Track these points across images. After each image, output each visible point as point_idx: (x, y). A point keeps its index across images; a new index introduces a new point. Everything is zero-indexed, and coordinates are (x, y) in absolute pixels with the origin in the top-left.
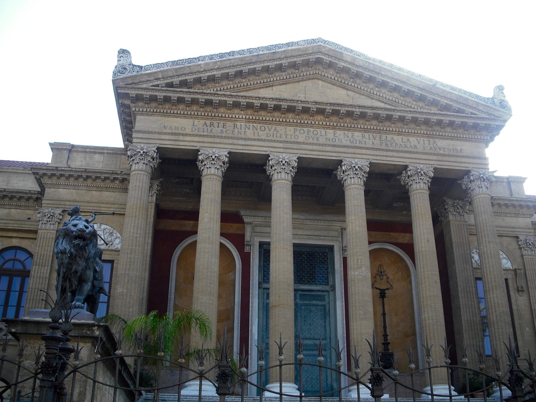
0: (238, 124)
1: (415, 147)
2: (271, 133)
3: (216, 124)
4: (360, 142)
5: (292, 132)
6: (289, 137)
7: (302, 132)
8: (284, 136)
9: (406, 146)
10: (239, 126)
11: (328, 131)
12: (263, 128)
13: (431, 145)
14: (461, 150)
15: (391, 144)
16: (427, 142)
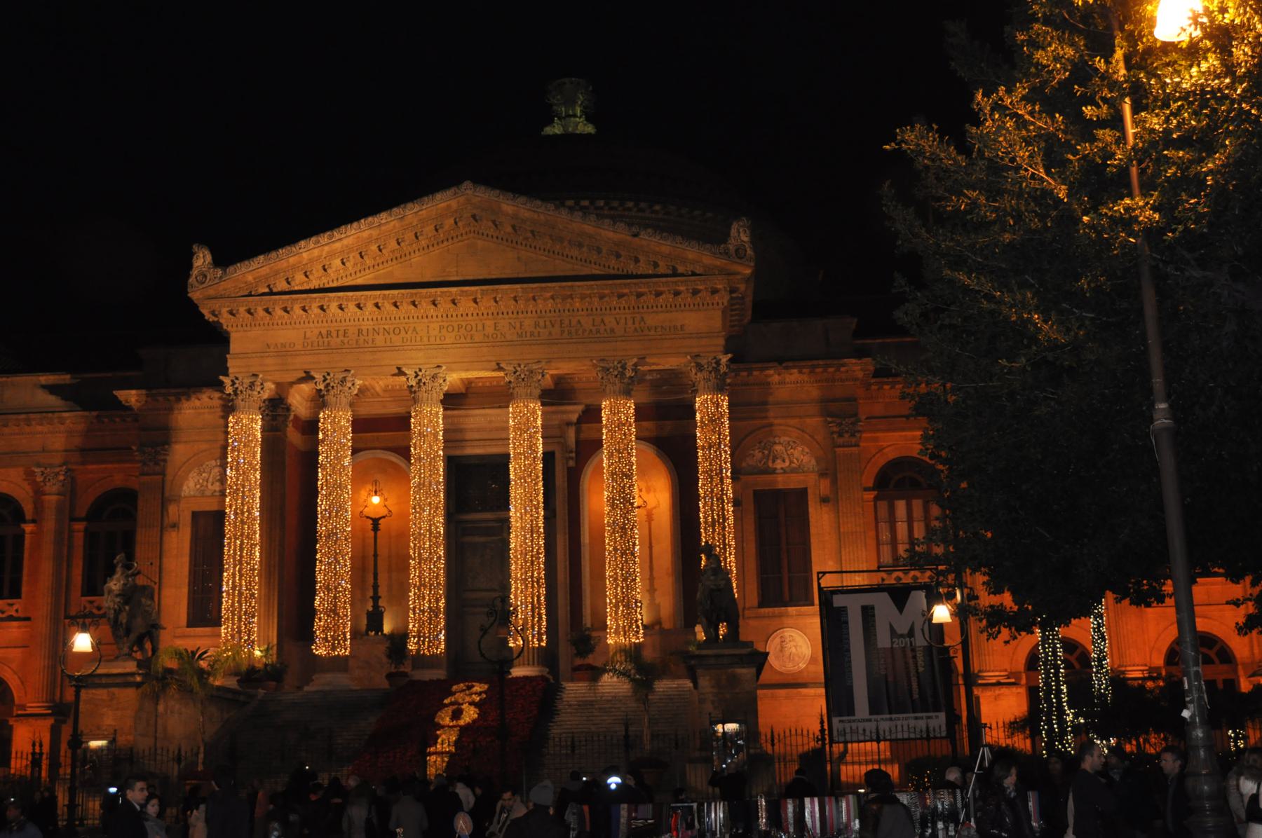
0: (364, 328)
1: (612, 330)
2: (408, 336)
3: (334, 334)
4: (532, 334)
5: (436, 332)
6: (432, 339)
7: (450, 329)
8: (425, 339)
9: (598, 332)
10: (365, 333)
11: (488, 323)
12: (397, 331)
13: (637, 325)
14: (682, 326)
15: (577, 331)
16: (630, 322)
